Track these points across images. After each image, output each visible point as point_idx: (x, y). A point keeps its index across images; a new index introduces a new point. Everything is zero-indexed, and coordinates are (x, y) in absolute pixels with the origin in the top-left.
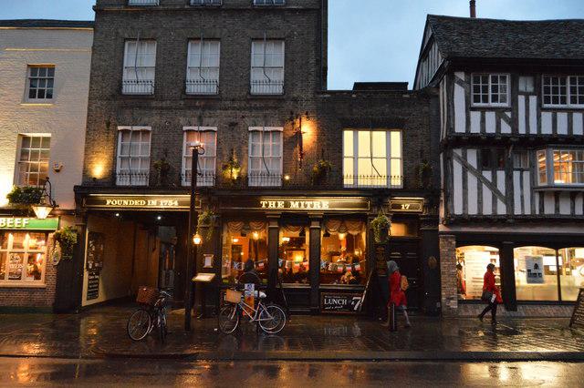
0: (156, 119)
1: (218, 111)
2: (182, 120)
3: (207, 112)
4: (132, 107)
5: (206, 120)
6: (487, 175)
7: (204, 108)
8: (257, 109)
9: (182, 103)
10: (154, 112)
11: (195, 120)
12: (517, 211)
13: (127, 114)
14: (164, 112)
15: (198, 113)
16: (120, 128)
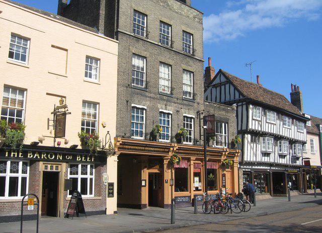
0: (148, 103)
1: (173, 104)
2: (159, 106)
3: (168, 103)
4: (138, 94)
5: (168, 107)
6: (252, 145)
7: (167, 101)
8: (185, 105)
9: (159, 96)
10: (147, 99)
11: (164, 106)
12: (257, 160)
13: (136, 98)
14: (152, 99)
15: (165, 102)
16: (133, 105)
